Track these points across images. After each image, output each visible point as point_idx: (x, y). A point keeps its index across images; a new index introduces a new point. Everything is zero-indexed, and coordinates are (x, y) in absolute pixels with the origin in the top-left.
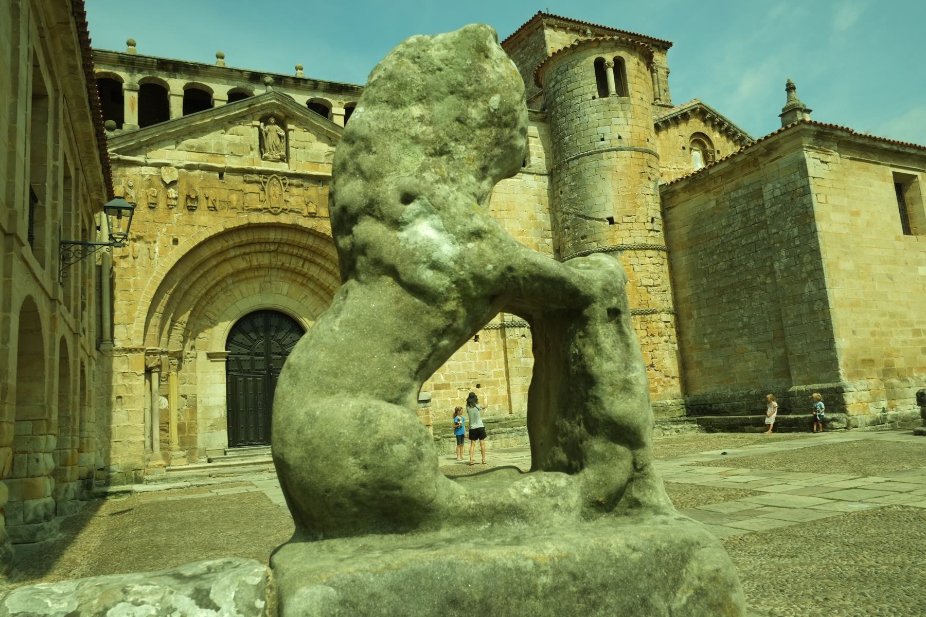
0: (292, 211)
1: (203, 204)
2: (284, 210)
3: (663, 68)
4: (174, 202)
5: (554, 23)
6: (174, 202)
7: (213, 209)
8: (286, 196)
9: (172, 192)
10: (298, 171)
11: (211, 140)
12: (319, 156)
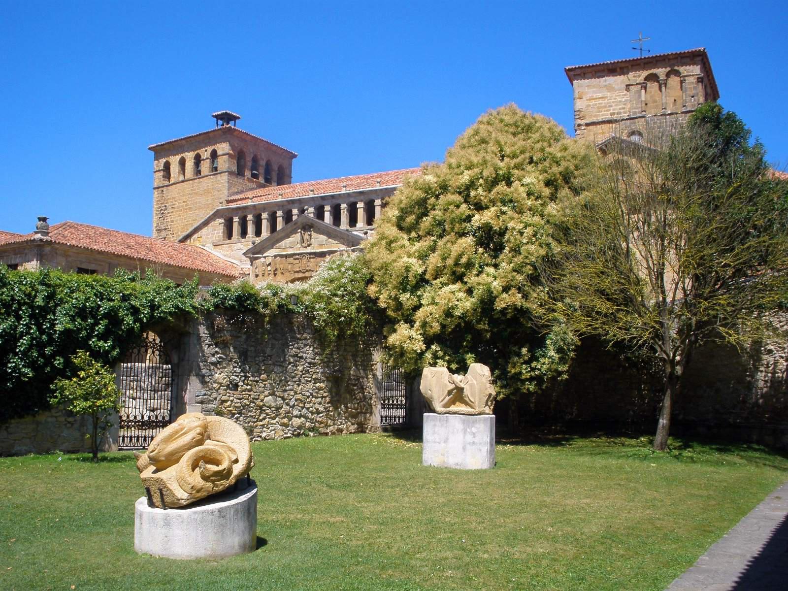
0: (310, 270)
1: (279, 272)
2: (307, 271)
3: (693, 75)
4: (270, 272)
5: (579, 73)
6: (270, 272)
7: (282, 274)
8: (308, 264)
9: (269, 268)
10: (312, 251)
11: (283, 243)
12: (323, 241)
